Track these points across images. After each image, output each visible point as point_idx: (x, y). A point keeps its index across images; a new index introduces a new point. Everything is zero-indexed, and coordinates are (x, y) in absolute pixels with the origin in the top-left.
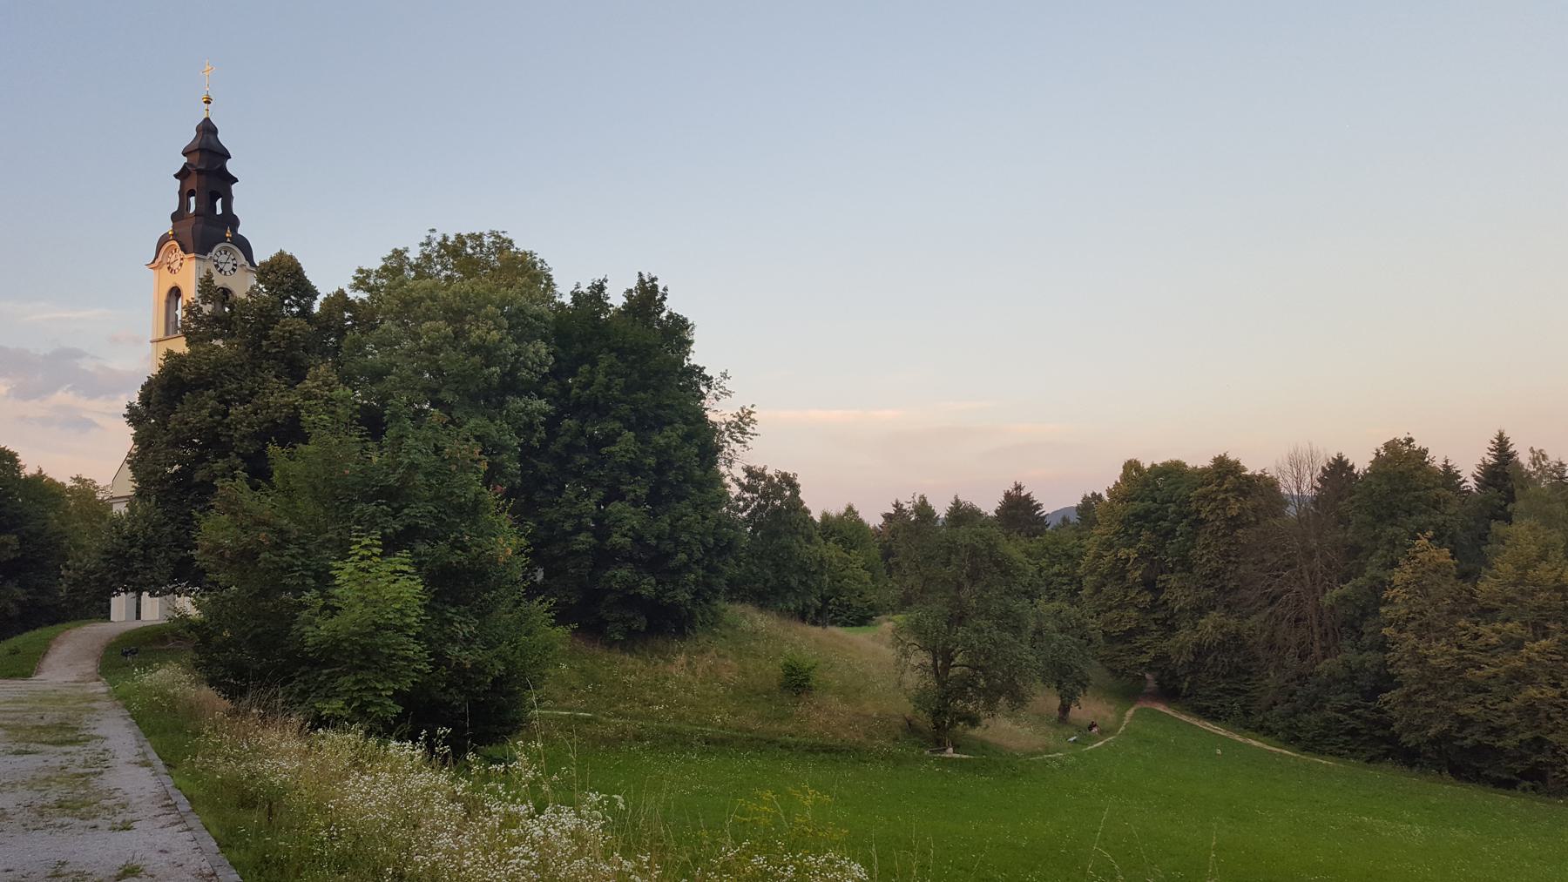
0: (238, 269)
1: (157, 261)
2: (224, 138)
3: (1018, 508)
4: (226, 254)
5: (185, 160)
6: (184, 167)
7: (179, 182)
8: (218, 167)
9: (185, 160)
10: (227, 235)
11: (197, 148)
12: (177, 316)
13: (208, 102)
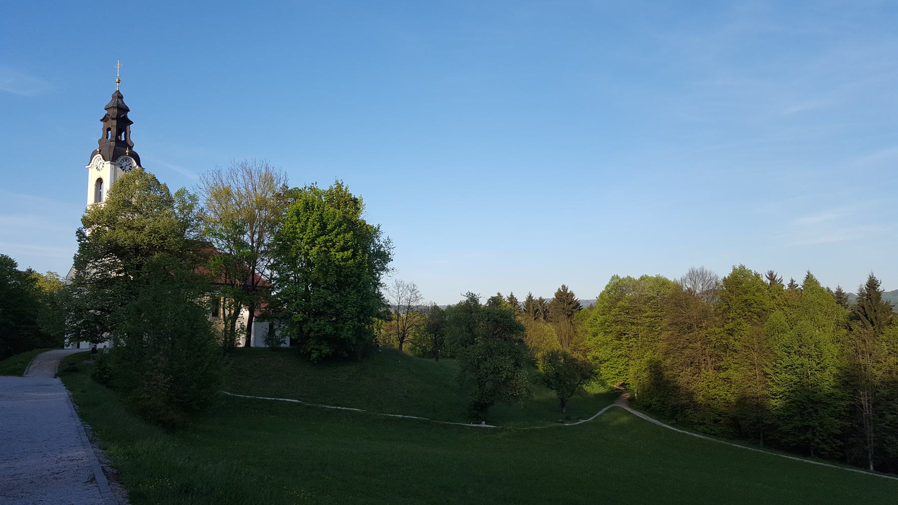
0: (132, 170)
1: (91, 164)
2: (127, 102)
3: (564, 298)
4: (126, 161)
5: (106, 112)
6: (105, 116)
7: (102, 123)
8: (122, 116)
9: (106, 112)
10: (127, 151)
11: (112, 106)
12: (100, 192)
13: (119, 82)
